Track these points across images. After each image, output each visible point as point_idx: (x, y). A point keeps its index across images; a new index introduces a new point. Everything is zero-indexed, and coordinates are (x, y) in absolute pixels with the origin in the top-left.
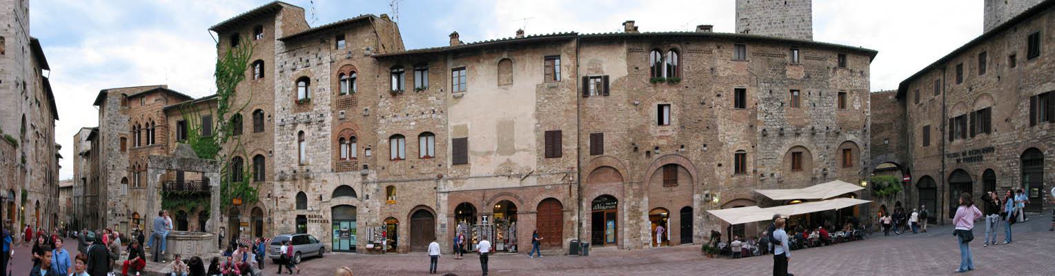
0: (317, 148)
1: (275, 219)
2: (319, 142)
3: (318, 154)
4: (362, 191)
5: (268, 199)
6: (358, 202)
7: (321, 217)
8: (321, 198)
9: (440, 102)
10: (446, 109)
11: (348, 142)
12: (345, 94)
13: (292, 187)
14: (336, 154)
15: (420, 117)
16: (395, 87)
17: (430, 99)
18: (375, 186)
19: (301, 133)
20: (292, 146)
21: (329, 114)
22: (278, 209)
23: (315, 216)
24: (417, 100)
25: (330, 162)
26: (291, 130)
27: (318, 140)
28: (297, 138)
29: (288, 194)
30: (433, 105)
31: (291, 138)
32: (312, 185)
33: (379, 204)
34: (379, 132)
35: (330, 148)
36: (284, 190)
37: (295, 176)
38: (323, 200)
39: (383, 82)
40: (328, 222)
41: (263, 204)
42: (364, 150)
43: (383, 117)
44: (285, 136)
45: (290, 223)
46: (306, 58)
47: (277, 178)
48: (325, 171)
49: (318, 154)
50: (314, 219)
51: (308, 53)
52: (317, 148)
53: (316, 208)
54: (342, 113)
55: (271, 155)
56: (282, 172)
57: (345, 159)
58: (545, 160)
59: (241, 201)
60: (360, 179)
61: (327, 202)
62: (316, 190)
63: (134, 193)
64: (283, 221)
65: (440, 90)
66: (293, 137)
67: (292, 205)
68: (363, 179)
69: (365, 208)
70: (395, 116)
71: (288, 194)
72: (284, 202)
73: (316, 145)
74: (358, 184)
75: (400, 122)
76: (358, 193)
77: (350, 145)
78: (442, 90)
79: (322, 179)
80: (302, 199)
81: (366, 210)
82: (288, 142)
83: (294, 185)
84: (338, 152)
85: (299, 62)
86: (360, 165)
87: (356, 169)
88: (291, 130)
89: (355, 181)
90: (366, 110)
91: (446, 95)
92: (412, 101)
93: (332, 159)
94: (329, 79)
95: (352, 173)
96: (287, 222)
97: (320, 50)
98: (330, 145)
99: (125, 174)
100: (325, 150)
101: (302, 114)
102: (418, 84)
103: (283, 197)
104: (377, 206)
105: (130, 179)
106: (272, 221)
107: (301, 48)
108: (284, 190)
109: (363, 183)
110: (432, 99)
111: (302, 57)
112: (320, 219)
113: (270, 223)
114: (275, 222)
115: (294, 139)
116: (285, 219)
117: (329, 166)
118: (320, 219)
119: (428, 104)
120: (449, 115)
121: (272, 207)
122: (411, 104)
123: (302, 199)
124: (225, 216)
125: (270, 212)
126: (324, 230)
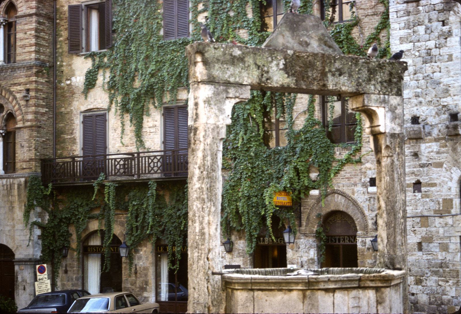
20: (444, 51)
26: (440, 11)
36: (422, 166)
37: (455, 127)
41: (355, 203)
44: (421, 29)
56: (415, 120)
64: (420, 244)
66: (446, 28)
67: (448, 202)
82: (431, 44)
88: (440, 11)
108: (422, 166)
116: (429, 239)
124: (241, 233)
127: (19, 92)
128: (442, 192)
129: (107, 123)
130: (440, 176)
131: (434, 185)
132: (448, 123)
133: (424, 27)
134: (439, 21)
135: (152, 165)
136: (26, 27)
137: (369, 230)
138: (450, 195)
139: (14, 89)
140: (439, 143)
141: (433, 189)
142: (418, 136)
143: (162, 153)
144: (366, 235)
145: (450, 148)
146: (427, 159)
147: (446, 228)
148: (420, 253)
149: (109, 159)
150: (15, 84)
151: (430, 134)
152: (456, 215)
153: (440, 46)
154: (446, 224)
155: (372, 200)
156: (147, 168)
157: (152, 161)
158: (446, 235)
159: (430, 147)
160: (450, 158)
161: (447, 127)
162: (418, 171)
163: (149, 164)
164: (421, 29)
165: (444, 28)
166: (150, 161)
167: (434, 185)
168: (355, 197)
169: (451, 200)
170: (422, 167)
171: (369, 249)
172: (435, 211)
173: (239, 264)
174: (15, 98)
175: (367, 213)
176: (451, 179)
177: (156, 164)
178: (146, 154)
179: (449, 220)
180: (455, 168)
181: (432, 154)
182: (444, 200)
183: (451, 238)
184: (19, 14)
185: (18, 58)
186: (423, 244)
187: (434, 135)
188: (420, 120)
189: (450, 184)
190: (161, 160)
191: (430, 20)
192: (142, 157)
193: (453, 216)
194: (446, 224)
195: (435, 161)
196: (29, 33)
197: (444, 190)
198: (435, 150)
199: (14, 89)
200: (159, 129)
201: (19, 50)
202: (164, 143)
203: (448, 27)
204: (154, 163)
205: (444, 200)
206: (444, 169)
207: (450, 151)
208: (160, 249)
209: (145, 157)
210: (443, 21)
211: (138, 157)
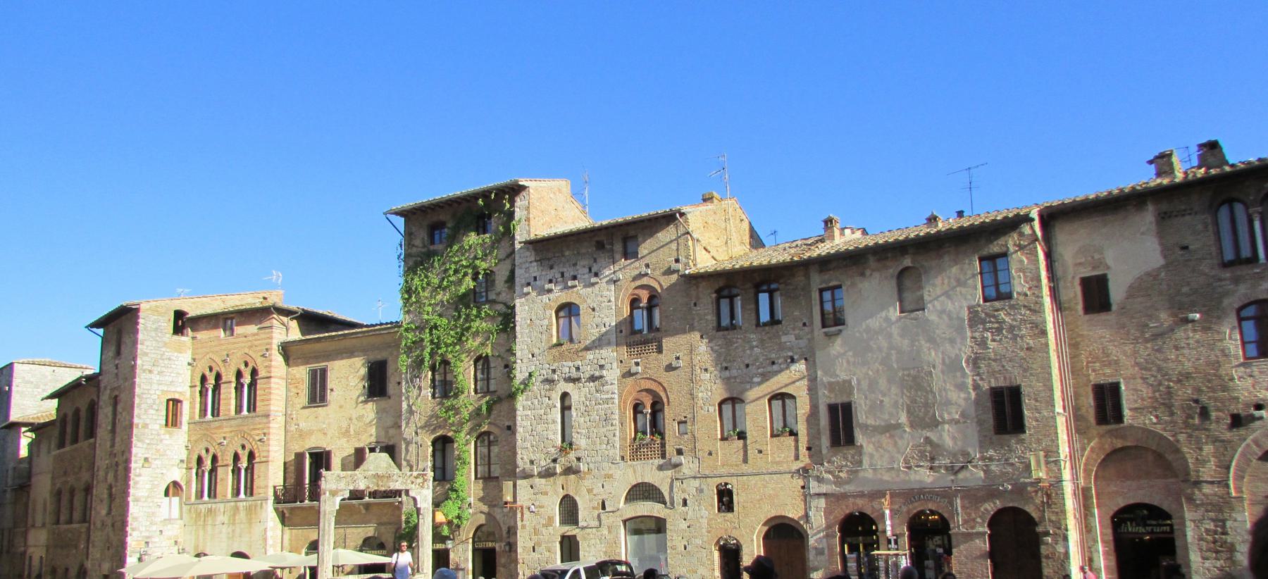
1: (520, 544)
9: (803, 343)
10: (814, 354)
12: (641, 331)
15: (769, 369)
16: (725, 321)
17: (784, 339)
18: (696, 483)
19: (565, 396)
21: (615, 365)
22: (524, 527)
24: (762, 341)
30: (790, 349)
31: (548, 405)
32: (587, 483)
33: (704, 513)
34: (700, 395)
39: (705, 315)
43: (706, 370)
46: (572, 273)
51: (575, 265)
54: (637, 364)
55: (509, 432)
58: (995, 438)
61: (613, 512)
62: (595, 492)
63: (198, 514)
65: (801, 325)
66: (550, 402)
70: (726, 368)
75: (735, 378)
78: (804, 324)
79: (603, 473)
80: (569, 510)
81: (684, 525)
85: (560, 279)
90: (678, 358)
91: (812, 331)
92: (754, 343)
94: (614, 307)
97: (595, 261)
99: (178, 474)
101: (564, 363)
102: (765, 316)
104: (702, 517)
105: (189, 482)
107: (563, 256)
110: (789, 339)
111: (565, 270)
113: (510, 551)
117: (617, 453)
119: (782, 347)
120: (817, 360)
121: (512, 524)
122: (752, 348)
123: (569, 510)
125: (509, 532)
127: (258, 435)
136: (265, 386)
139: (253, 433)
141: (542, 509)
144: (501, 541)
150: (254, 429)
164: (536, 402)
168: (495, 514)
171: (503, 551)
174: (254, 439)
184: (260, 376)
185: (257, 409)
186: (536, 547)
196: (267, 391)
199: (253, 433)
201: (258, 404)
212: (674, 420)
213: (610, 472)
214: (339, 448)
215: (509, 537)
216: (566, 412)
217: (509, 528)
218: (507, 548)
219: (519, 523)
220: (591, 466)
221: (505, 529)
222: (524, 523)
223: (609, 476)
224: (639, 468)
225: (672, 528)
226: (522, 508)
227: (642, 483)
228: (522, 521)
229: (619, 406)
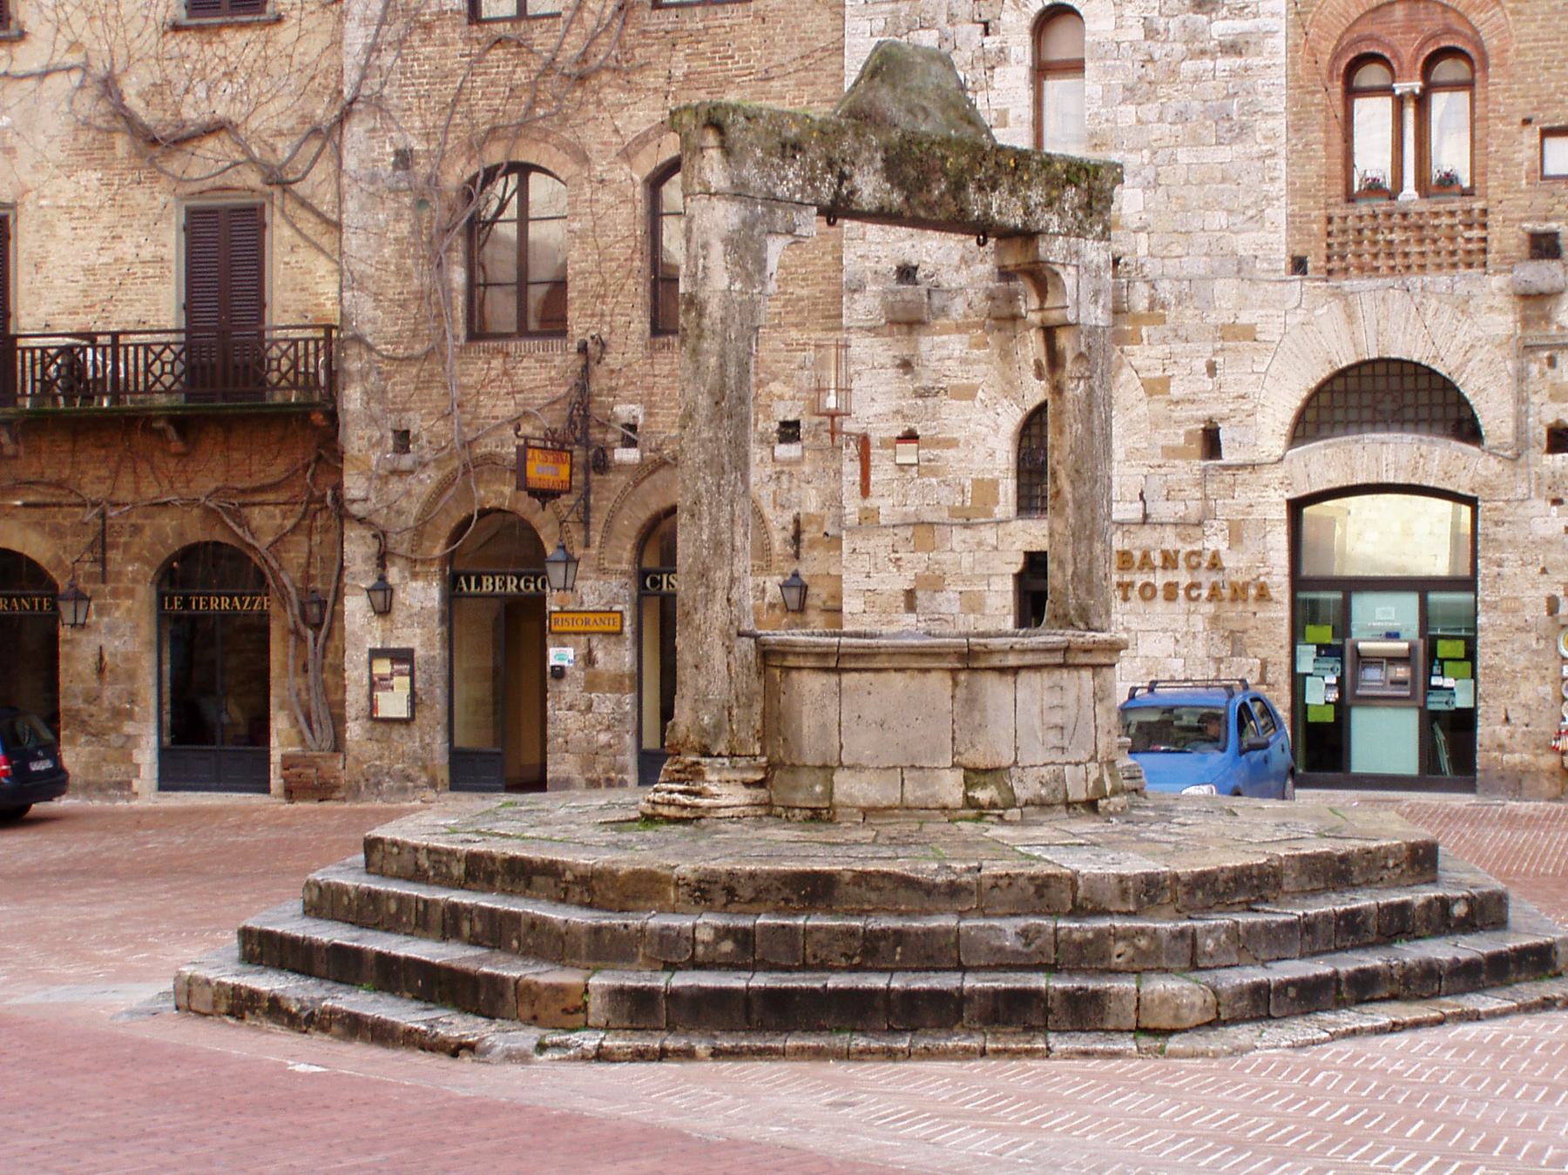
0: (1182, 117)
1: (852, 582)
2: (1197, 79)
3: (1183, 156)
4: (1521, 400)
5: (786, 451)
6: (1494, 465)
7: (1215, 565)
8: (1211, 442)
11: (1416, 85)
13: (984, 373)
14: (1322, 159)
22: (869, 519)
23: (1169, 561)
25: (1278, 214)
27: (1188, 67)
28: (1021, 49)
29: (952, 417)
35: (1280, 124)
36: (923, 393)
37: (1011, 298)
38: (1228, 457)
40: (1263, 595)
42: (1531, 137)
45: (973, 603)
47: (863, 308)
48: (1242, 268)
49: (1183, 156)
50: (1160, 579)
52: (1182, 117)
53: (1180, 508)
56: (907, 273)
57: (1392, 196)
59: (564, 471)
60: (1504, 323)
62: (1176, 390)
64: (910, 595)
66: (991, 43)
68: (1526, 322)
69: (1540, 505)
71: (952, 417)
72: (926, 469)
73: (1176, 97)
74: (1481, 354)
76: (1494, 412)
77: (1422, 102)
79: (1213, 318)
83: (1006, 355)
84: (1337, 137)
86: (1506, 236)
87: (1477, 258)
89: (1466, 332)
93: (1296, 191)
95: (1442, 281)
96: (948, 602)
98: (1279, 103)
100: (1241, 132)
103: (910, 437)
106: (818, 596)
108: (923, 393)
109: (1530, 349)
112: (1206, 578)
114: (851, 605)
115: (1002, 55)
118: (1206, 578)
121: (811, 502)
124: (416, 566)
125: (797, 538)
126: (1237, 642)
128: (972, 461)
129: (11, 244)
130: (968, 421)
131: (952, 443)
132: (991, 285)
133: (935, 33)
134: (974, 22)
135: (156, 368)
137: (775, 558)
138: (991, 471)
140: (966, 337)
141: (950, 453)
142: (913, 317)
143: (182, 337)
145: (996, 351)
146: (935, 376)
147: (980, 554)
148: (911, 618)
149: (24, 350)
151: (944, 311)
152: (1008, 521)
153: (977, 86)
154: (980, 544)
155: (784, 478)
156: (141, 379)
157: (158, 356)
158: (978, 570)
159: (943, 345)
160: (993, 376)
161: (991, 297)
162: (912, 407)
163: (148, 366)
165: (986, 40)
166: (151, 357)
167: (952, 443)
169: (995, 484)
170: (921, 396)
171: (772, 606)
172: (953, 511)
173: (411, 645)
175: (769, 512)
176: (996, 429)
177: (168, 368)
178: (135, 339)
179: (989, 535)
180: (1006, 402)
181: (948, 363)
182: (977, 483)
183: (992, 579)
186: (919, 594)
187: (954, 315)
188: (920, 275)
189: (992, 442)
190: (183, 356)
191: (952, 18)
192: (126, 346)
193: (998, 523)
194: (980, 544)
195: (955, 382)
197: (976, 458)
198: (956, 354)
200: (173, 268)
202: (189, 307)
203: (998, 39)
204: (163, 364)
205: (977, 483)
206: (978, 404)
207: (996, 357)
208: (171, 603)
209: (136, 346)
210: (986, 24)
211: (115, 345)
212: (1527, 122)
213: (1245, 318)
214: (68, 210)
215: (797, 556)
216: (1054, 87)
217: (797, 521)
218: (794, 595)
219: (852, 507)
220: (1166, 289)
221: (779, 523)
222: (872, 502)
223: (1238, 333)
224: (1367, 306)
225: (1502, 533)
226: (864, 442)
227: (1380, 360)
228: (865, 491)
229: (1292, 63)
